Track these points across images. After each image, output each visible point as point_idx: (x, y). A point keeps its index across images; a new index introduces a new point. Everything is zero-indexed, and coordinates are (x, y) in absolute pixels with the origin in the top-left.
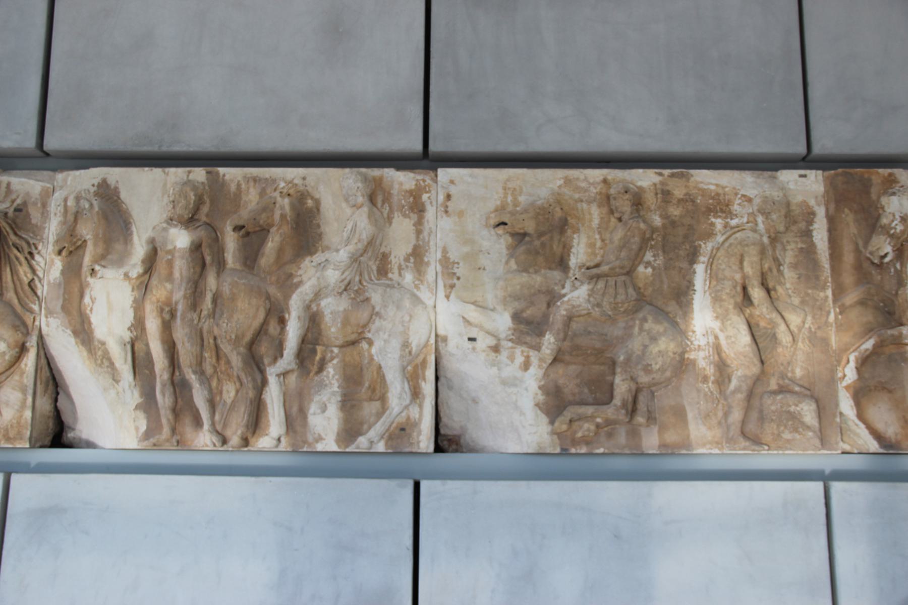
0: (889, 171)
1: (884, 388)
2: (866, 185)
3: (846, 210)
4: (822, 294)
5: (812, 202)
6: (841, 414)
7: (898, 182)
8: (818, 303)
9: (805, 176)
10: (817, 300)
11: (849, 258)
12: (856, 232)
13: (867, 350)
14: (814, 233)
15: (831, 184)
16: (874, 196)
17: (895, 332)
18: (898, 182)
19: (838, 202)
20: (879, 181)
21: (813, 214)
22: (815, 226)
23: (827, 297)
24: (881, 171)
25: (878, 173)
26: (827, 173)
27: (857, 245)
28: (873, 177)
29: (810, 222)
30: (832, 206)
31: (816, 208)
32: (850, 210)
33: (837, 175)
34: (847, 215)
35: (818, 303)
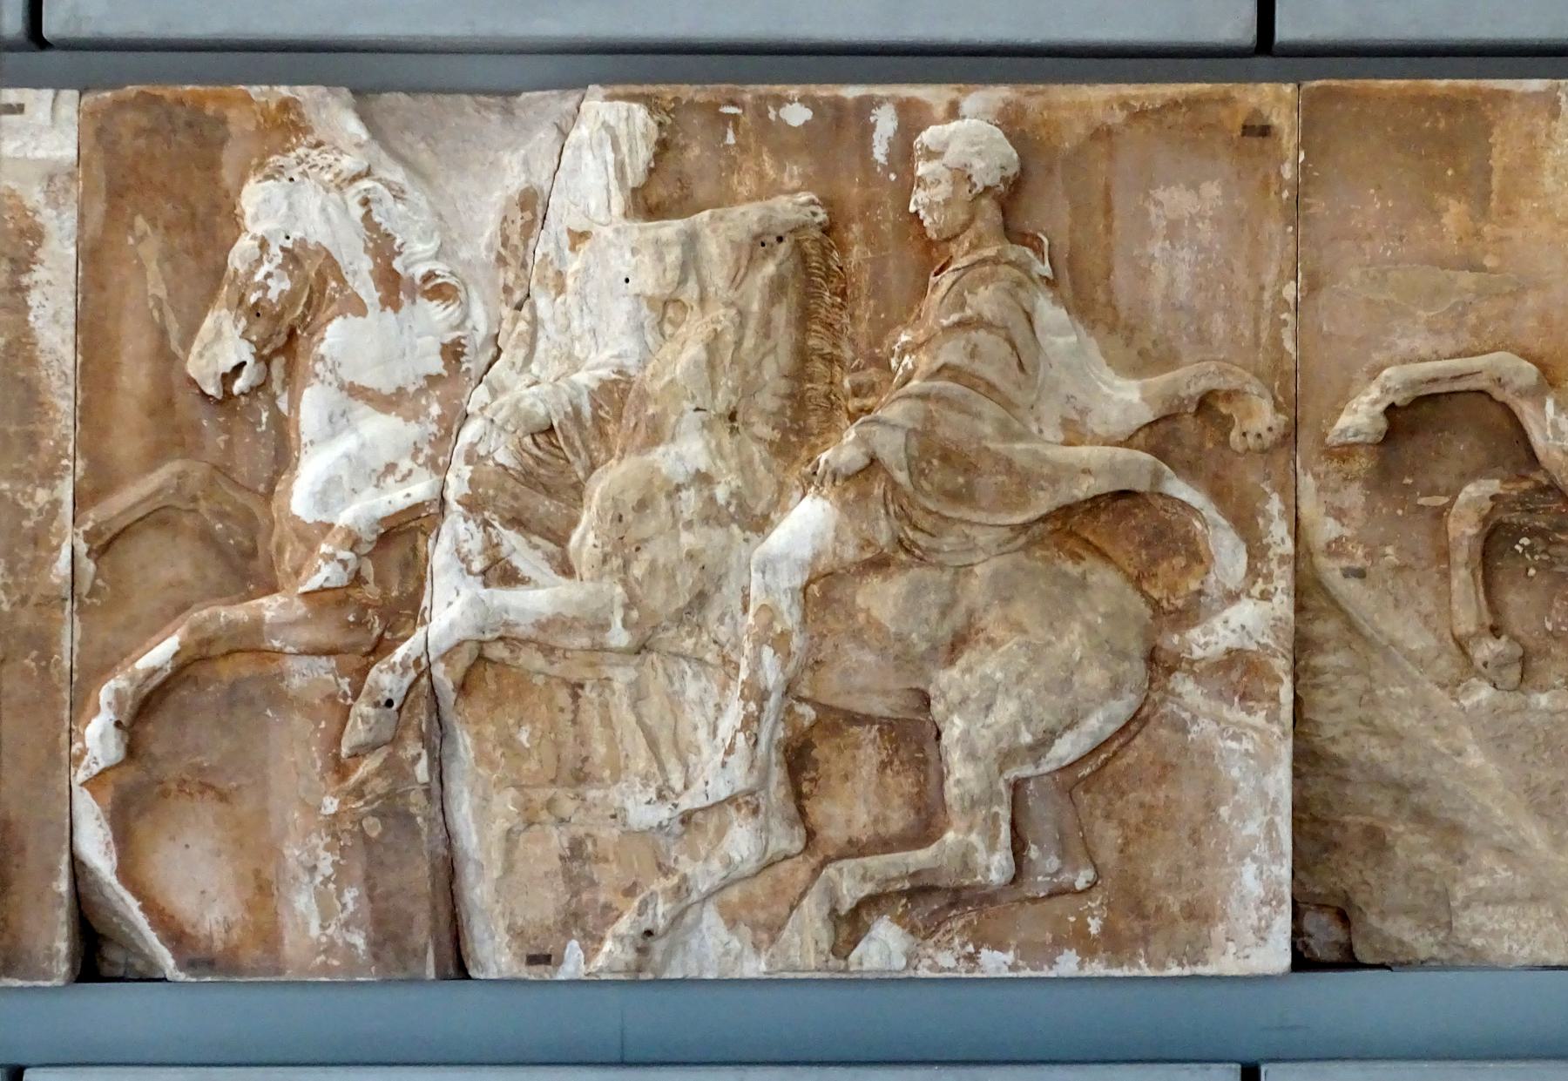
0: (284, 91)
1: (206, 787)
2: (203, 140)
3: (140, 222)
4: (42, 496)
5: (35, 196)
6: (78, 867)
7: (308, 130)
8: (27, 524)
9: (19, 109)
10: (26, 514)
11: (134, 378)
12: (162, 292)
13: (153, 672)
14: (34, 298)
15: (100, 132)
16: (228, 176)
17: (240, 613)
18: (308, 130)
19: (116, 194)
20: (251, 127)
21: (36, 234)
22: (39, 274)
23: (56, 504)
24: (255, 90)
25: (248, 99)
26: (89, 98)
27: (163, 333)
28: (232, 114)
29: (22, 264)
30: (99, 208)
31: (47, 217)
32: (152, 221)
33: (120, 105)
34: (141, 239)
35: (27, 524)
